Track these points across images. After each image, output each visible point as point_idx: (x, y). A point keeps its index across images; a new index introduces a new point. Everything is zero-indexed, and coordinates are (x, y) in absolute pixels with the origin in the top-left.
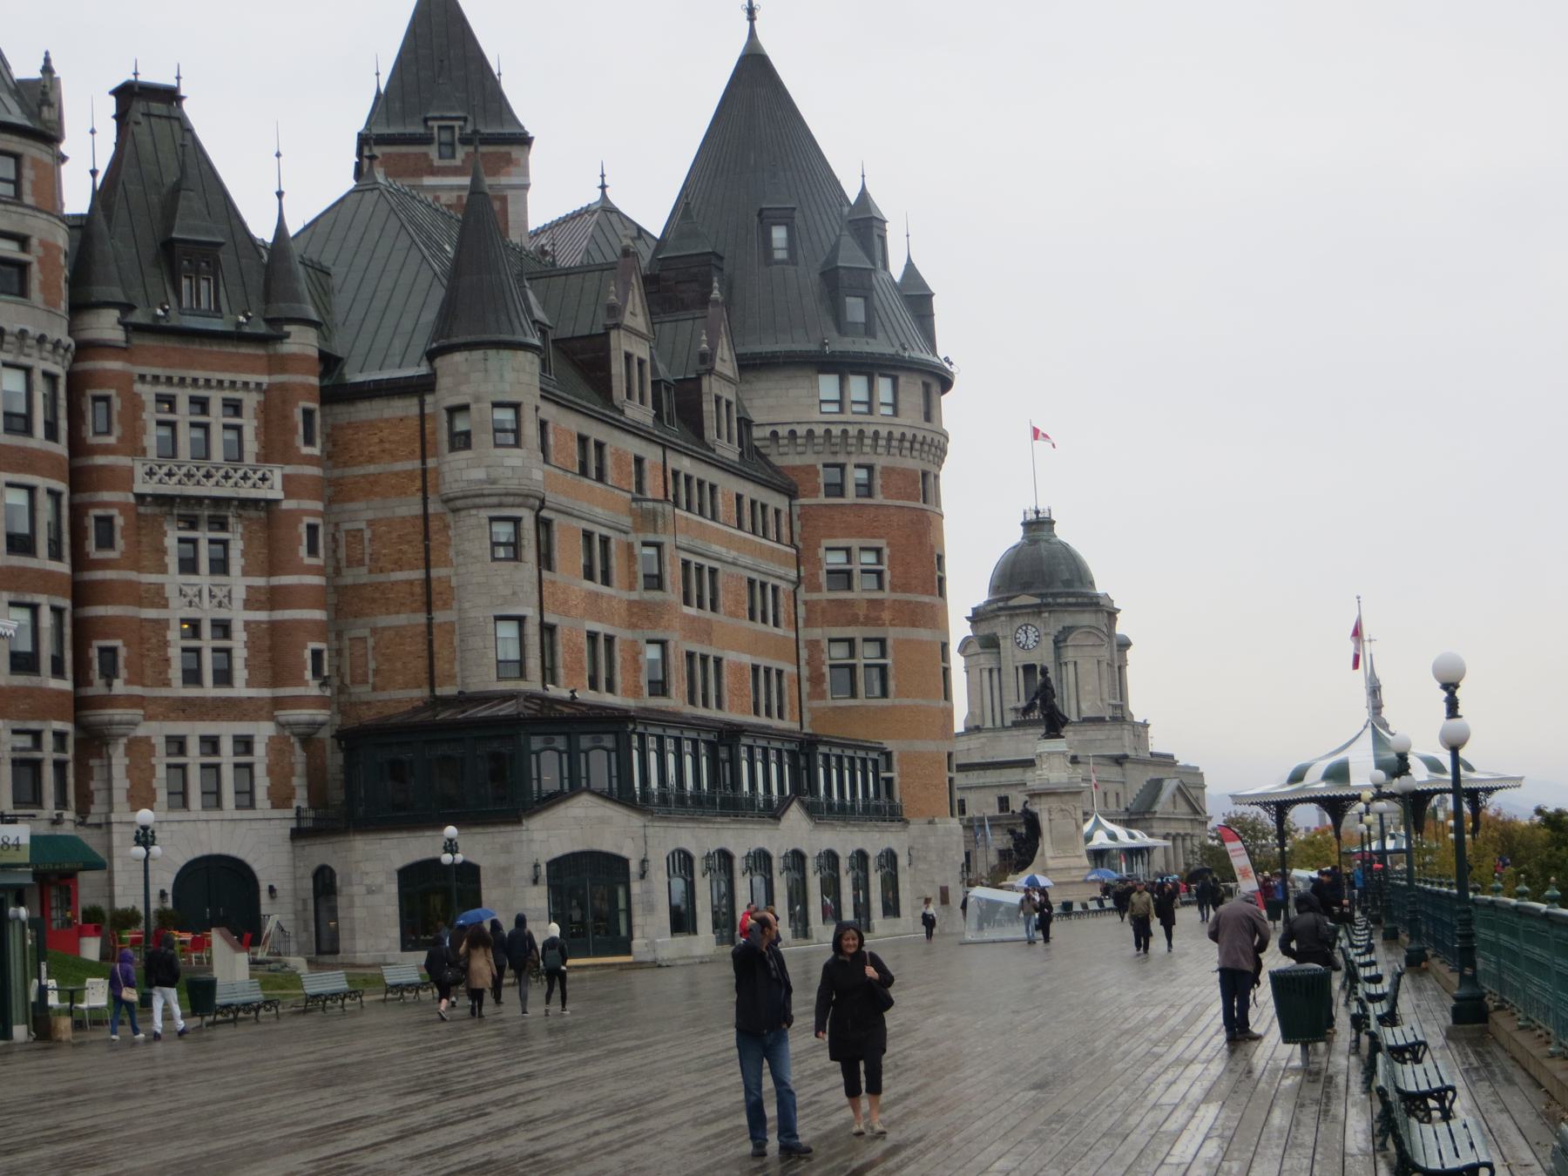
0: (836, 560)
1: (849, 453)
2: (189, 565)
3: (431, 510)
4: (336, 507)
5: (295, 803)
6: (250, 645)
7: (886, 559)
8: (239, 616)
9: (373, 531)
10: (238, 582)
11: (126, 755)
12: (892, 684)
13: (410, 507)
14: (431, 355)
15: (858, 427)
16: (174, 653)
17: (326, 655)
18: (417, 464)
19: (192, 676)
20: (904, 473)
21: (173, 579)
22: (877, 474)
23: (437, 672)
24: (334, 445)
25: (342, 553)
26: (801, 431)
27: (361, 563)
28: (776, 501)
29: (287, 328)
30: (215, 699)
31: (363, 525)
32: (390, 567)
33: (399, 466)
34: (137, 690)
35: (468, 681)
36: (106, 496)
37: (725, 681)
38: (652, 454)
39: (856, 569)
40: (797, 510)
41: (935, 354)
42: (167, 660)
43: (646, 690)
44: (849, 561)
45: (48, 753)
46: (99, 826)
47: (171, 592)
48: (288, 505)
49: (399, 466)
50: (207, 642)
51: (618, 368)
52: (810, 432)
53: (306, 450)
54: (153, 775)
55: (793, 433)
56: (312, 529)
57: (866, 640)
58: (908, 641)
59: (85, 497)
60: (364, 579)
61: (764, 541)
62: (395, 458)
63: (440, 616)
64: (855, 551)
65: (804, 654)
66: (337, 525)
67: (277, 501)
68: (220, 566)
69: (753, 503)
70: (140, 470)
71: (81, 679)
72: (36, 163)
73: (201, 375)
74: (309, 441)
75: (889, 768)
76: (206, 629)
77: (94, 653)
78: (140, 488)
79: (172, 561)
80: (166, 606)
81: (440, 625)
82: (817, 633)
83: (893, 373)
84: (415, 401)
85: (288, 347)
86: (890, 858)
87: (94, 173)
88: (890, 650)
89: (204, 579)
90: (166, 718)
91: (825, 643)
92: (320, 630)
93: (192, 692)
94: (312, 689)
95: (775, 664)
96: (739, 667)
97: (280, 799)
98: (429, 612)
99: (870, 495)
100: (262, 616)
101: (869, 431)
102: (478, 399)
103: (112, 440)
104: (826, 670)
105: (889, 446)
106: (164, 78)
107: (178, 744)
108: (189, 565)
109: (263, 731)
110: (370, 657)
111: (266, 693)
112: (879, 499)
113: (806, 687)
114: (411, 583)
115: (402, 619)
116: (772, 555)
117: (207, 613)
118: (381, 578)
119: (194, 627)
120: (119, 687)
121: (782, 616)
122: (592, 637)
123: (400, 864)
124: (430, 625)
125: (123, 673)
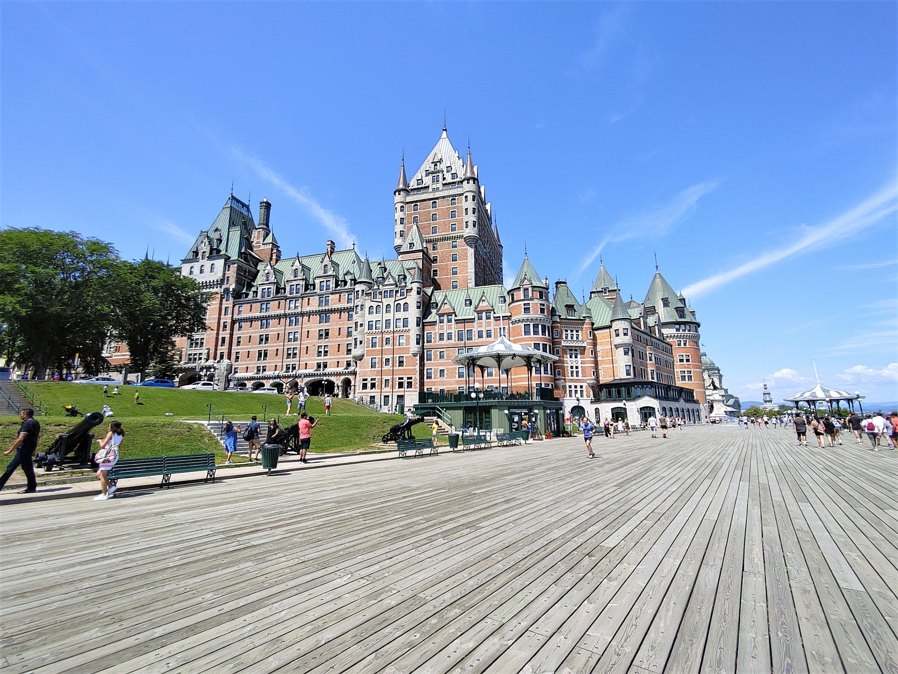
8: (580, 365)
14: (611, 321)
19: (572, 375)
47: (569, 362)
48: (588, 347)
50: (574, 370)
56: (592, 351)
68: (576, 357)
70: (563, 342)
71: (555, 376)
72: (545, 293)
76: (574, 368)
78: (563, 344)
93: (572, 378)
108: (571, 357)
109: (585, 385)
115: (608, 366)
117: (574, 365)
119: (572, 367)
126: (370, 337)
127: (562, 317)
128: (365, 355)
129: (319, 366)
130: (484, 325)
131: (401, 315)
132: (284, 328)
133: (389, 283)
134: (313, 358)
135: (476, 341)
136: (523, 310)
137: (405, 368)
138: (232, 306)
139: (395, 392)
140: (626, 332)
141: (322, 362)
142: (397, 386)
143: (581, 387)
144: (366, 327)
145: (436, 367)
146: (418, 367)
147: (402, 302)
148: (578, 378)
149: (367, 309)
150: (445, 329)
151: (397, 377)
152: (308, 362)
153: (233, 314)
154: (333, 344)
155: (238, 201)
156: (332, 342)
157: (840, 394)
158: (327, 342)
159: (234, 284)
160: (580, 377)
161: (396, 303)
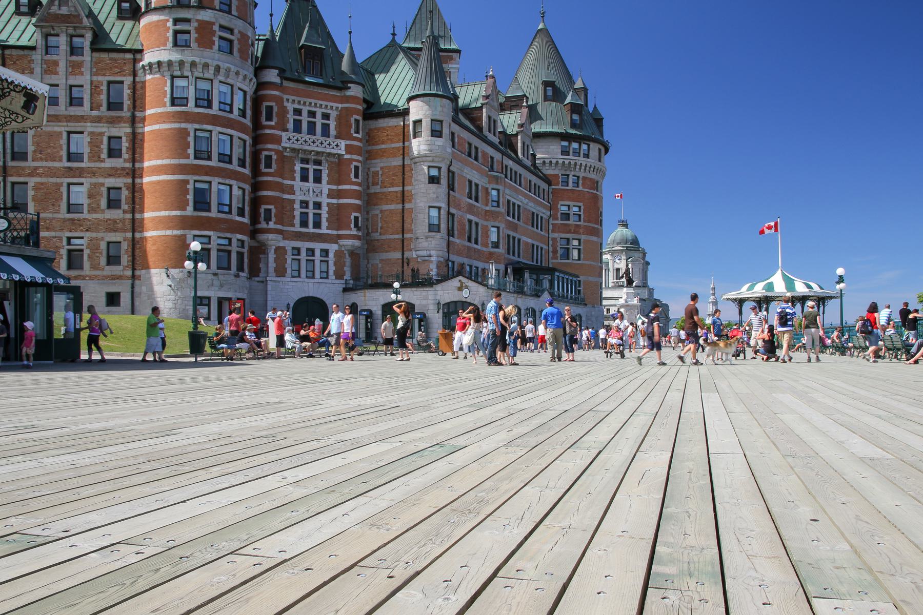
0: (564, 209)
1: (571, 171)
2: (304, 178)
3: (405, 163)
4: (368, 162)
5: (345, 278)
7: (582, 210)
8: (325, 201)
9: (383, 172)
10: (325, 187)
11: (275, 253)
12: (582, 256)
13: (398, 162)
15: (575, 161)
16: (297, 213)
17: (360, 219)
18: (401, 144)
19: (304, 224)
20: (591, 180)
21: (297, 184)
22: (580, 179)
23: (405, 229)
24: (369, 137)
25: (370, 180)
26: (554, 161)
27: (377, 184)
28: (544, 185)
29: (349, 85)
30: (313, 233)
31: (379, 169)
32: (389, 185)
33: (394, 145)
34: (279, 227)
35: (417, 232)
36: (270, 146)
37: (521, 247)
38: (497, 156)
39: (571, 213)
40: (551, 190)
41: (602, 136)
42: (294, 216)
43: (490, 246)
44: (569, 210)
45: (234, 248)
46: (262, 282)
47: (296, 188)
49: (394, 145)
52: (557, 162)
54: (286, 263)
55: (551, 162)
56: (357, 168)
58: (589, 241)
59: (260, 146)
60: (378, 191)
61: (538, 198)
62: (392, 142)
63: (407, 206)
64: (571, 206)
65: (551, 242)
66: (369, 169)
67: (343, 155)
68: (318, 180)
69: (535, 184)
70: (285, 135)
73: (313, 101)
74: (357, 132)
75: (579, 286)
76: (311, 205)
77: (262, 211)
78: (283, 145)
79: (298, 176)
80: (294, 194)
81: (407, 209)
82: (556, 235)
83: (588, 143)
84: (401, 119)
85: (350, 93)
89: (310, 184)
90: (292, 240)
91: (558, 239)
92: (358, 208)
93: (304, 230)
94: (354, 232)
95: (541, 245)
96: (527, 243)
97: (339, 275)
98: (403, 204)
99: (578, 187)
100: (334, 201)
101: (579, 163)
103: (273, 123)
105: (585, 169)
108: (304, 178)
110: (379, 221)
111: (335, 232)
112: (580, 188)
113: (551, 254)
114: (396, 192)
115: (392, 207)
116: (541, 204)
117: (311, 198)
118: (385, 190)
120: (272, 225)
121: (543, 228)
122: (470, 221)
123: (383, 303)
124: (403, 209)
125: (274, 219)
127: (288, 75)
140: (438, 128)
143: (325, 252)
157: (809, 287)
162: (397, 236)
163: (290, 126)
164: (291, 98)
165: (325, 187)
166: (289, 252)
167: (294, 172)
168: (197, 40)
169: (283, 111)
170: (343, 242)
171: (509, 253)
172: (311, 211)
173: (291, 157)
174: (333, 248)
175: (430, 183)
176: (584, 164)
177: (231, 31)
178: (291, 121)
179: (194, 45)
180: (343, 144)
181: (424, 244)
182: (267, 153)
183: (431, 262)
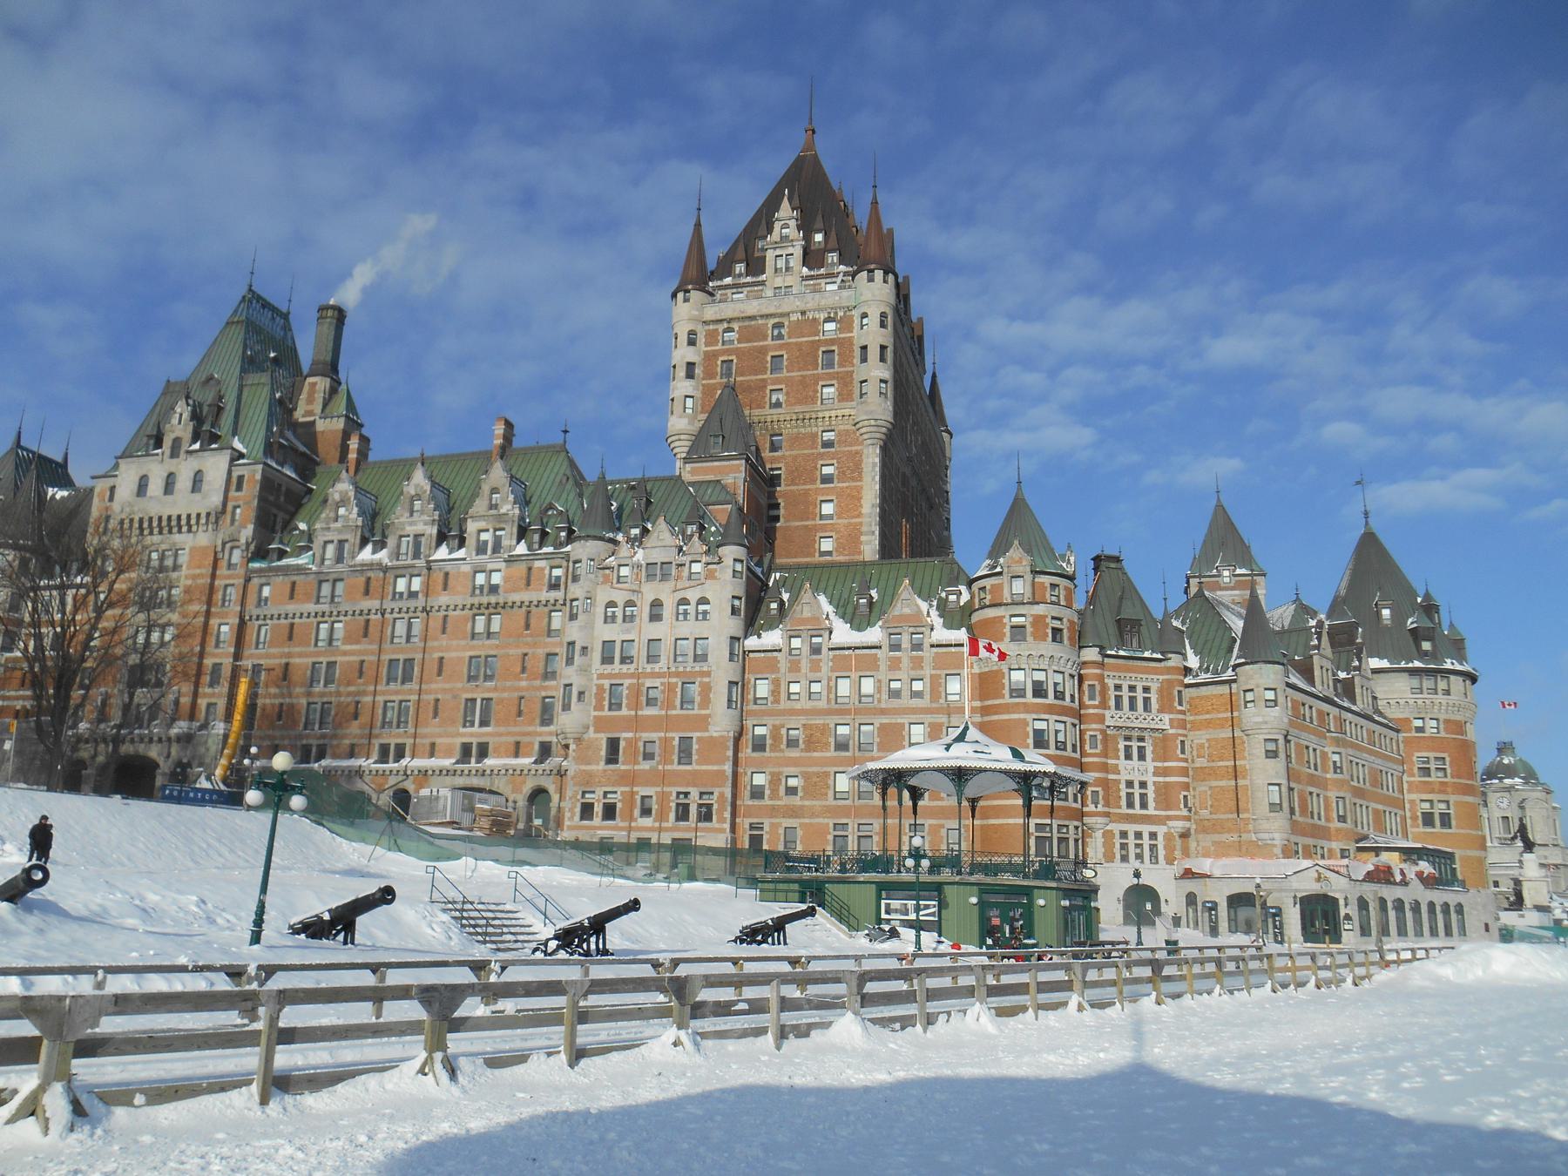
6: (1156, 792)
8: (1151, 779)
10: (1150, 764)
19: (1130, 805)
22: (1441, 723)
26: (1402, 702)
29: (1170, 655)
33: (1221, 715)
34: (1106, 809)
40: (1401, 739)
48: (1171, 731)
49: (1221, 715)
51: (1317, 673)
53: (1180, 708)
56: (1182, 742)
57: (1439, 801)
63: (1241, 782)
65: (1407, 806)
68: (1142, 757)
70: (1108, 714)
73: (1134, 675)
76: (1136, 785)
79: (1122, 754)
82: (1414, 796)
86: (1460, 909)
87: (1087, 592)
88: (1451, 806)
89: (1135, 761)
91: (1418, 802)
93: (1131, 811)
94: (1185, 812)
100: (1161, 779)
102: (1258, 686)
104: (1419, 814)
106: (1111, 551)
107: (1124, 834)
108: (1128, 757)
111: (1163, 813)
113: (1409, 821)
114: (1227, 767)
115: (1223, 783)
119: (1130, 784)
120: (1100, 808)
122: (1311, 793)
126: (606, 683)
128: (592, 729)
129: (466, 751)
130: (905, 663)
131: (689, 628)
132: (375, 647)
133: (660, 544)
134: (451, 729)
135: (883, 705)
136: (1007, 630)
137: (698, 768)
138: (242, 581)
139: (667, 830)
141: (474, 741)
142: (672, 816)
143: (1153, 835)
144: (596, 656)
145: (776, 770)
146: (728, 768)
147: (693, 596)
148: (1144, 812)
149: (600, 610)
150: (803, 671)
151: (674, 790)
152: (438, 741)
153: (243, 604)
154: (505, 695)
155: (266, 305)
156: (504, 690)
158: (489, 690)
159: (251, 527)
160: (1151, 810)
161: (680, 595)
162: (1231, 816)
163: (1112, 703)
164: (1111, 674)
165: (1150, 764)
166: (1117, 835)
167: (1118, 750)
168: (1033, 634)
169: (1104, 687)
170: (1170, 823)
171: (1356, 826)
172: (1137, 791)
173: (1114, 735)
174: (1161, 830)
175: (1267, 757)
176: (1444, 702)
177: (1060, 619)
178: (1113, 698)
179: (1029, 638)
180: (1166, 717)
181: (1265, 825)
182: (1092, 733)
183: (1275, 846)
